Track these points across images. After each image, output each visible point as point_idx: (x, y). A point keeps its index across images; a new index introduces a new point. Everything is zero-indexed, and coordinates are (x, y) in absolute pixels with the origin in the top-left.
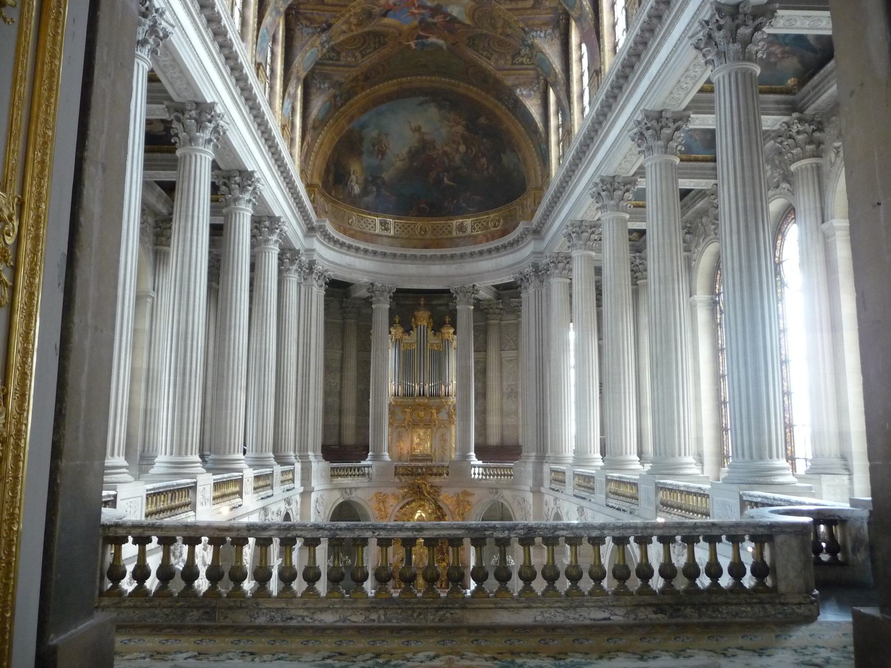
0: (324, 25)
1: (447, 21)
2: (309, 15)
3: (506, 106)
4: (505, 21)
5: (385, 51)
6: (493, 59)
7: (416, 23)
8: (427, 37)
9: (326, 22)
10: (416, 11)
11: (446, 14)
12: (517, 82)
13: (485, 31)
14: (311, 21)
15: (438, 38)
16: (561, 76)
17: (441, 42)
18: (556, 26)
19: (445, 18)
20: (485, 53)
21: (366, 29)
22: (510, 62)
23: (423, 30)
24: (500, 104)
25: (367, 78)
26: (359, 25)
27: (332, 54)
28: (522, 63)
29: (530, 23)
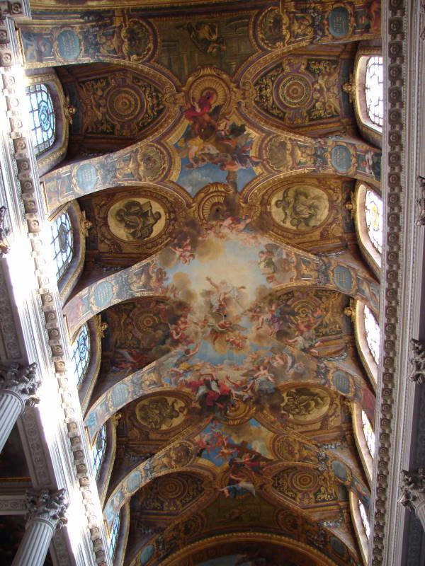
0: (148, 455)
1: (252, 461)
2: (136, 448)
3: (320, 549)
4: (300, 443)
5: (202, 499)
6: (298, 500)
7: (227, 465)
8: (238, 482)
9: (150, 453)
10: (226, 451)
11: (252, 452)
12: (323, 517)
13: (286, 463)
14: (138, 452)
15: (247, 481)
16: (356, 471)
17: (250, 486)
18: (343, 439)
19: (251, 457)
20: (290, 494)
21: (184, 469)
22: (313, 500)
23: (234, 473)
24: (311, 548)
25: (187, 531)
26: (177, 461)
27: (157, 504)
28: (324, 500)
29: (320, 440)
